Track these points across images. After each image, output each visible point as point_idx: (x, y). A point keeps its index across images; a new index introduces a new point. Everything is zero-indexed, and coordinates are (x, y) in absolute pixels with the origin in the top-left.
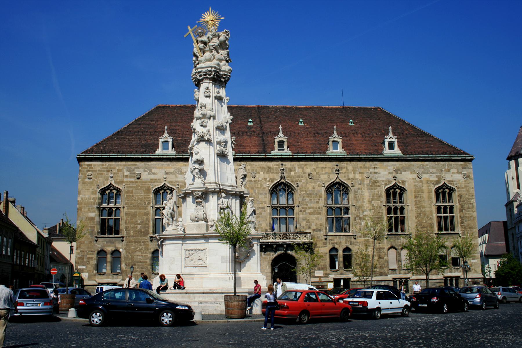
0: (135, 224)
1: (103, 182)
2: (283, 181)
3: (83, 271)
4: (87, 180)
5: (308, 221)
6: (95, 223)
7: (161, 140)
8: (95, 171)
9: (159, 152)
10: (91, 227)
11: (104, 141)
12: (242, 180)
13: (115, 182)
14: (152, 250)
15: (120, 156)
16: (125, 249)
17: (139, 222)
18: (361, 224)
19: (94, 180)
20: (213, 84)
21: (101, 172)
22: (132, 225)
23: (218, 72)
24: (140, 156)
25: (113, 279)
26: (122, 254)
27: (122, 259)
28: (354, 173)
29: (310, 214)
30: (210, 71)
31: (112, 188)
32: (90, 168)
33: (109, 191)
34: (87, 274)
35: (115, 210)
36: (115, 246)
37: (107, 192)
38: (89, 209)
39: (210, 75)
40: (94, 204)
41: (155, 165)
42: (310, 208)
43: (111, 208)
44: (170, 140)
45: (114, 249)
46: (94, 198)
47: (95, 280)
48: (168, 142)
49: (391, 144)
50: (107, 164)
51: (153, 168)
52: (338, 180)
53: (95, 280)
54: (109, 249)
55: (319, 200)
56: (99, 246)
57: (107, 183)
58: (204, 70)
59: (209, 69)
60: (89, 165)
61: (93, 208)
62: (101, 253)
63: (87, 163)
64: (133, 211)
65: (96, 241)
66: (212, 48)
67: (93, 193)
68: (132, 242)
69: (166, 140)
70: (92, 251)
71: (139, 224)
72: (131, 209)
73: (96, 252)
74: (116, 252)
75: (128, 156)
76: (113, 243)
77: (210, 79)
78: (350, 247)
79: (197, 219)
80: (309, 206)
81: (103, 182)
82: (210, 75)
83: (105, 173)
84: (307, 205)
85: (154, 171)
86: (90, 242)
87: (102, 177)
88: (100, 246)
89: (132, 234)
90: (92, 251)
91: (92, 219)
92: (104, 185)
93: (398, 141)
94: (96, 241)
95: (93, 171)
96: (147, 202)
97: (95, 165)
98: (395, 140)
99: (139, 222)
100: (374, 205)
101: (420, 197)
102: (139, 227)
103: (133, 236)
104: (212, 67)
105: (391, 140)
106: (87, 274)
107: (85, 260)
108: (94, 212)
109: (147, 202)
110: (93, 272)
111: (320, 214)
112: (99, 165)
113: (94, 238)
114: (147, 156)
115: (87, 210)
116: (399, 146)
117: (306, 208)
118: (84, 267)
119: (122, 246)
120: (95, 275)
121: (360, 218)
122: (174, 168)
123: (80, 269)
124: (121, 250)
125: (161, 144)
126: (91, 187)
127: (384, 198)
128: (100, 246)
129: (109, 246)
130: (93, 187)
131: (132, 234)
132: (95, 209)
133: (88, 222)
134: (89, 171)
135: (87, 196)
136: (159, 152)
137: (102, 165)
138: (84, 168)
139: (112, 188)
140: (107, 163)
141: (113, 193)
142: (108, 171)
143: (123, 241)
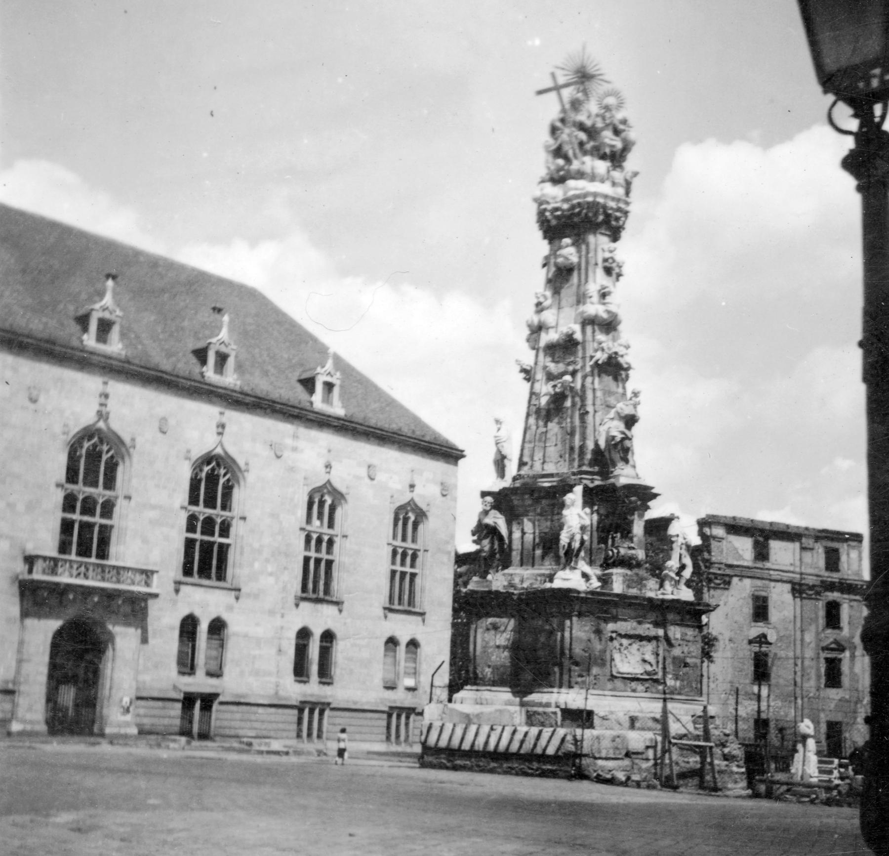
2: (101, 425)
5: (145, 541)
42: (154, 507)
52: (219, 451)
105: (329, 379)
111: (173, 527)
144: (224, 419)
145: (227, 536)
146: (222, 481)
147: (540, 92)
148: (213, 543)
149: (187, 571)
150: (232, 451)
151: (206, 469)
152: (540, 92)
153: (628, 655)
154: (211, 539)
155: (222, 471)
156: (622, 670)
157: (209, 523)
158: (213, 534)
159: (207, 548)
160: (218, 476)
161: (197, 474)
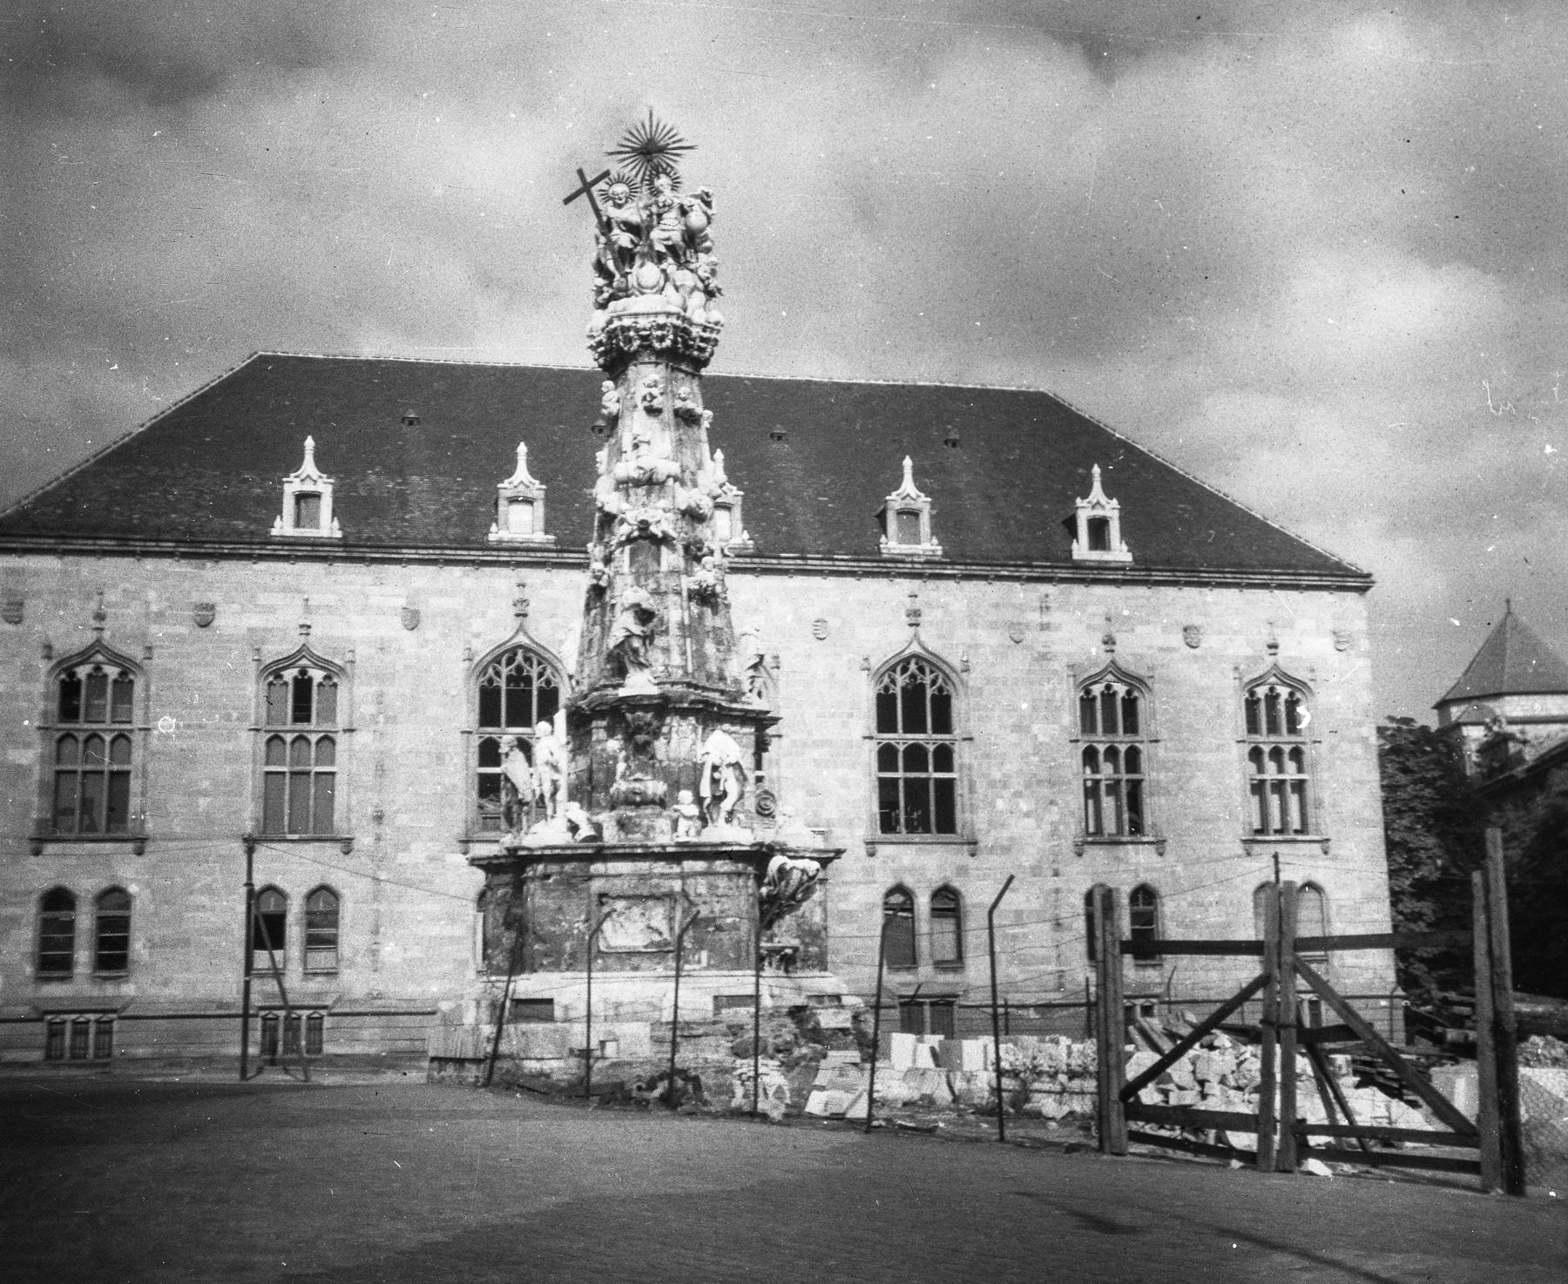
6: (34, 787)
9: (284, 526)
12: (751, 673)
16: (148, 885)
18: (992, 804)
23: (685, 330)
26: (137, 905)
27: (137, 921)
28: (973, 625)
29: (817, 763)
30: (661, 327)
31: (100, 658)
35: (113, 742)
39: (661, 339)
43: (94, 735)
45: (105, 884)
49: (1098, 528)
52: (915, 648)
54: (86, 885)
55: (851, 715)
56: (45, 871)
58: (643, 322)
59: (661, 320)
62: (58, 900)
66: (663, 250)
67: (28, 674)
71: (206, 794)
73: (35, 897)
74: (114, 899)
77: (660, 354)
78: (956, 884)
79: (638, 799)
80: (817, 736)
82: (661, 339)
84: (810, 733)
85: (262, 599)
91: (21, 771)
93: (1121, 518)
96: (235, 715)
98: (1111, 509)
100: (1041, 738)
101: (1196, 713)
102: (203, 802)
104: (669, 314)
105: (1099, 512)
108: (27, 745)
109: (235, 715)
111: (853, 766)
116: (1124, 535)
117: (805, 745)
121: (992, 784)
124: (133, 889)
125: (288, 504)
127: (1070, 717)
128: (47, 873)
132: (36, 737)
136: (284, 526)
137: (65, 573)
141: (105, 676)
144: (918, 604)
145: (950, 769)
146: (929, 692)
147: (567, 201)
148: (927, 780)
149: (888, 823)
150: (934, 645)
151: (901, 680)
152: (567, 201)
153: (626, 924)
154: (923, 775)
155: (928, 679)
156: (613, 944)
157: (915, 756)
158: (926, 770)
159: (916, 790)
160: (922, 686)
161: (886, 688)
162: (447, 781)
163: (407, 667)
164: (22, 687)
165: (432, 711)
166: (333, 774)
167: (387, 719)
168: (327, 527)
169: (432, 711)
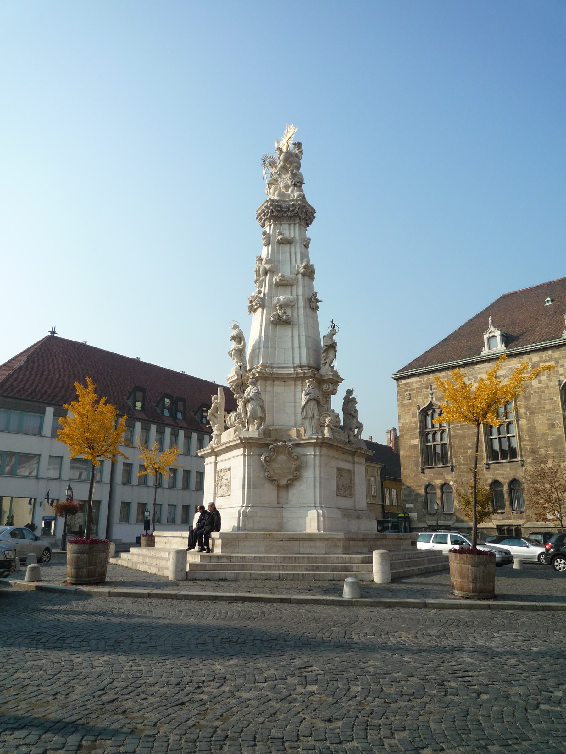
0: (464, 449)
1: (423, 401)
3: (410, 510)
4: (406, 402)
7: (486, 336)
8: (413, 390)
9: (485, 352)
10: (415, 457)
11: (426, 352)
13: (436, 399)
14: (490, 481)
15: (437, 366)
16: (456, 482)
17: (469, 445)
19: (413, 400)
20: (275, 225)
21: (419, 390)
22: (461, 451)
24: (460, 362)
25: (445, 520)
31: (434, 407)
32: (408, 387)
33: (431, 411)
34: (416, 514)
36: (444, 478)
37: (430, 413)
38: (411, 435)
40: (416, 429)
41: (482, 369)
44: (498, 333)
45: (443, 482)
46: (415, 421)
47: (425, 522)
48: (495, 337)
50: (425, 380)
51: (479, 373)
53: (425, 522)
54: (438, 482)
57: (428, 402)
60: (406, 384)
61: (415, 434)
63: (404, 381)
64: (460, 432)
65: (423, 472)
67: (414, 416)
68: (464, 472)
69: (492, 334)
70: (419, 486)
71: (470, 448)
72: (458, 429)
73: (424, 487)
75: (447, 364)
76: (442, 474)
81: (423, 401)
83: (424, 390)
86: (416, 475)
87: (421, 396)
88: (426, 479)
89: (462, 462)
90: (419, 486)
91: (415, 446)
92: (424, 404)
94: (423, 472)
95: (411, 390)
97: (412, 383)
99: (469, 445)
102: (470, 451)
103: (464, 464)
106: (416, 514)
107: (413, 497)
108: (417, 438)
110: (422, 511)
112: (416, 382)
113: (420, 470)
114: (469, 360)
115: (408, 437)
118: (412, 506)
119: (452, 477)
120: (425, 515)
122: (505, 369)
123: (408, 508)
124: (451, 483)
126: (410, 410)
129: (437, 479)
130: (413, 408)
131: (462, 462)
133: (412, 450)
134: (407, 390)
135: (407, 421)
137: (420, 381)
138: (402, 388)
139: (434, 407)
140: (425, 378)
142: (427, 387)
143: (452, 470)
162: (557, 434)
163: (536, 392)
164: (413, 420)
165: (547, 407)
166: (514, 436)
167: (531, 413)
168: (499, 347)
169: (547, 407)
